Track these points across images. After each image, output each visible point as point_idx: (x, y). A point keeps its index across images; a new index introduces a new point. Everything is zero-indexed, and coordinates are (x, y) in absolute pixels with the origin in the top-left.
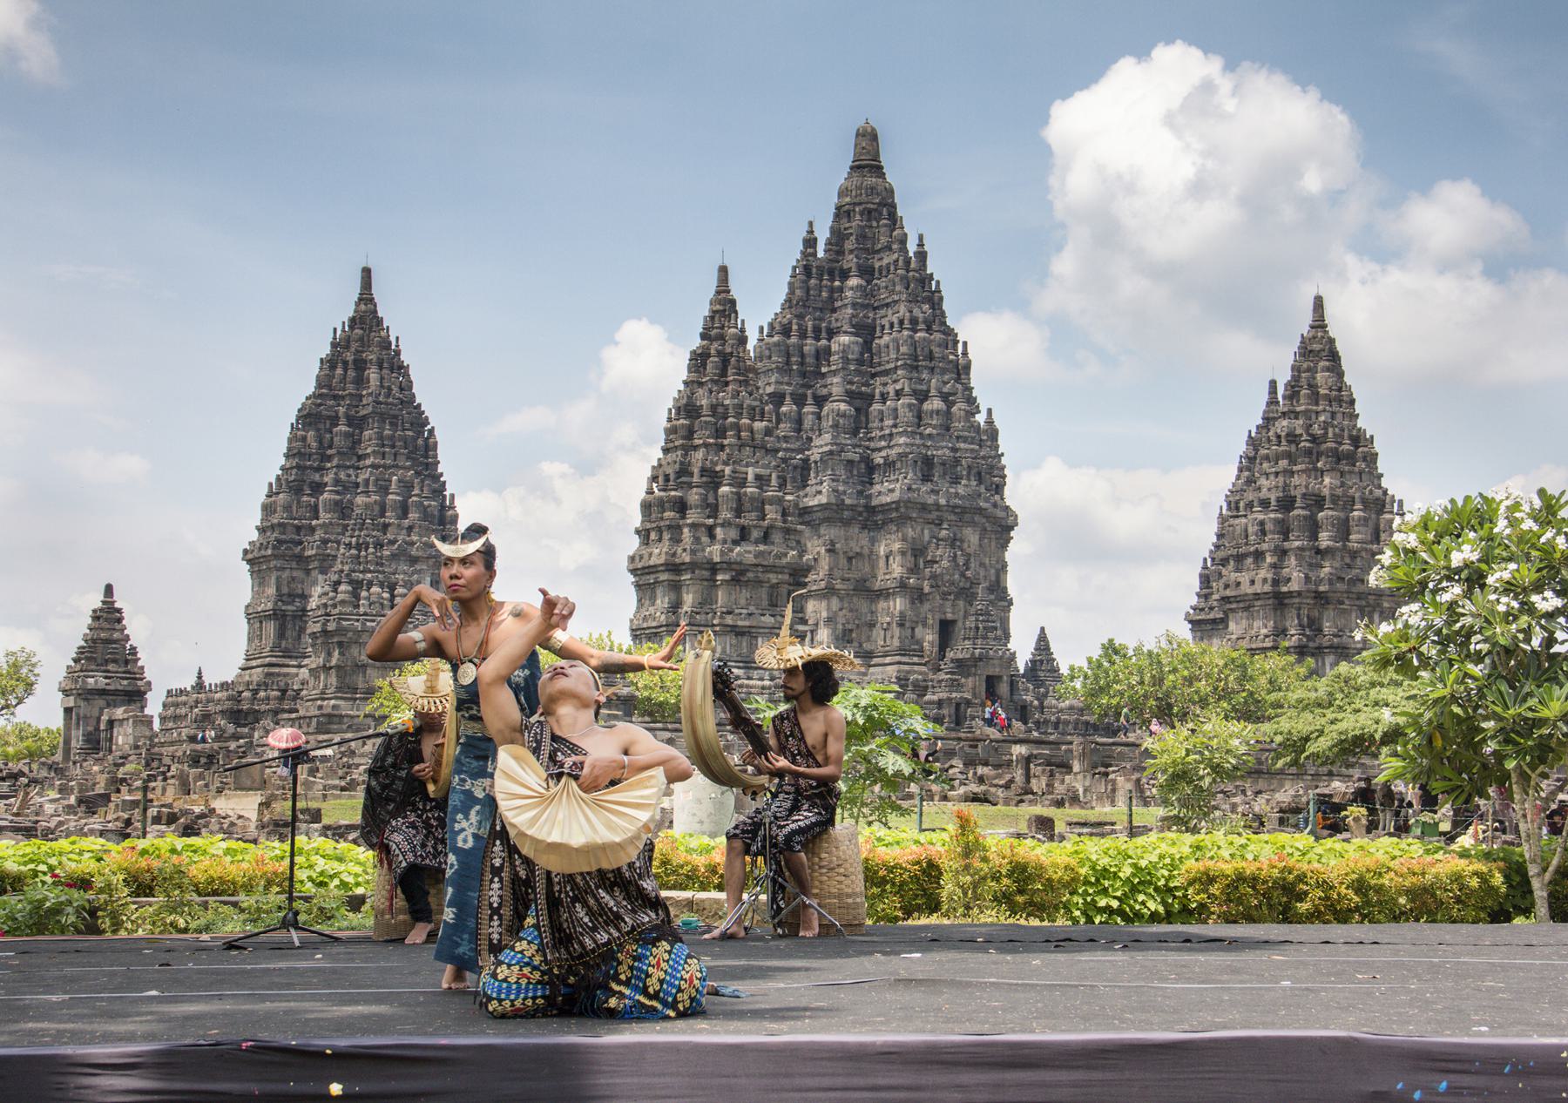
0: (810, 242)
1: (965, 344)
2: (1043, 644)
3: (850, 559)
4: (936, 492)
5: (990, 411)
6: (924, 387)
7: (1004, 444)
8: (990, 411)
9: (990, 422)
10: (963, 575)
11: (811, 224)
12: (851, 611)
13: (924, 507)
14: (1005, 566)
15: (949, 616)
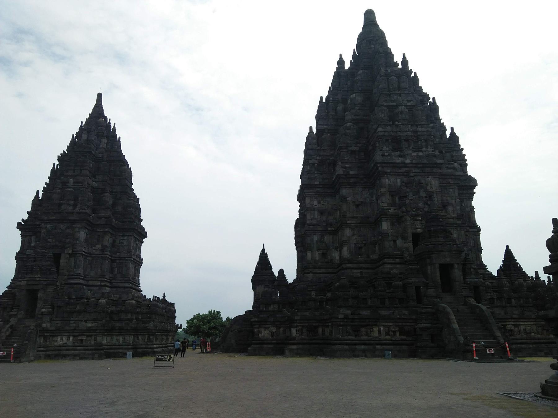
0: (341, 62)
1: (434, 99)
2: (508, 254)
3: (357, 206)
4: (404, 156)
5: (452, 129)
6: (394, 104)
7: (463, 143)
8: (452, 129)
9: (453, 133)
10: (426, 203)
11: (341, 55)
12: (359, 236)
13: (395, 165)
14: (473, 209)
15: (419, 230)
